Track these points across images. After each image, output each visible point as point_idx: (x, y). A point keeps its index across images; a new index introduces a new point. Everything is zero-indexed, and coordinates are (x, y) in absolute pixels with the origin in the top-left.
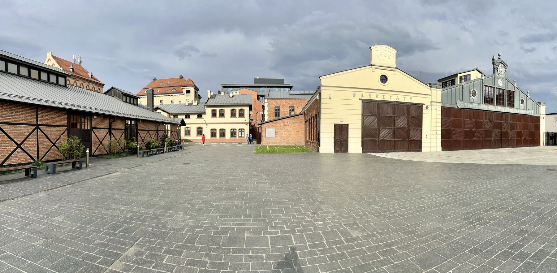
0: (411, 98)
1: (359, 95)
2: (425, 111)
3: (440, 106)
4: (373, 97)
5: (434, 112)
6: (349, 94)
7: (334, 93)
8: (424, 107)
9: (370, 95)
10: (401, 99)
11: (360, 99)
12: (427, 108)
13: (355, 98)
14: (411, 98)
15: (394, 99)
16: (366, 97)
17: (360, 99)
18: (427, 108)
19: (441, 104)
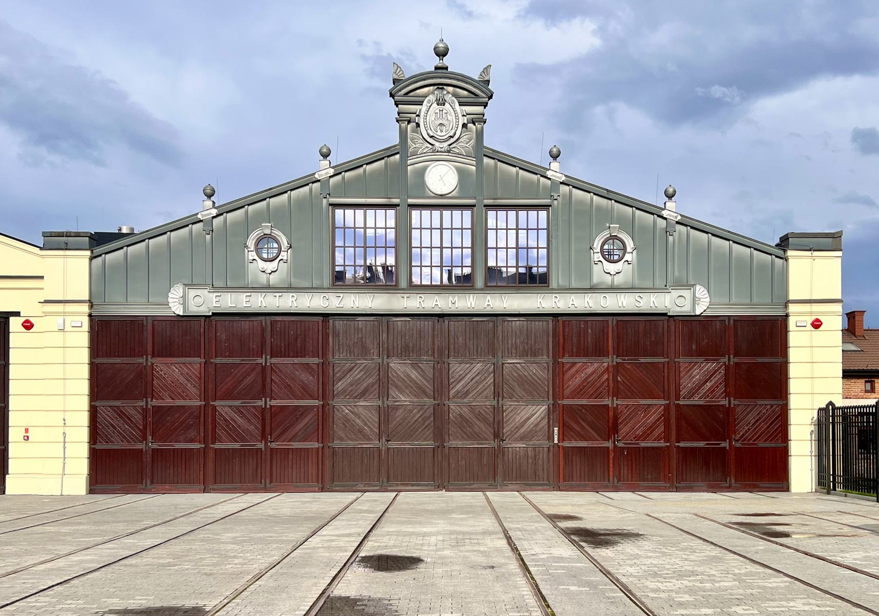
3: (80, 318)
8: (15, 324)
12: (28, 325)
18: (28, 325)
19: (85, 308)
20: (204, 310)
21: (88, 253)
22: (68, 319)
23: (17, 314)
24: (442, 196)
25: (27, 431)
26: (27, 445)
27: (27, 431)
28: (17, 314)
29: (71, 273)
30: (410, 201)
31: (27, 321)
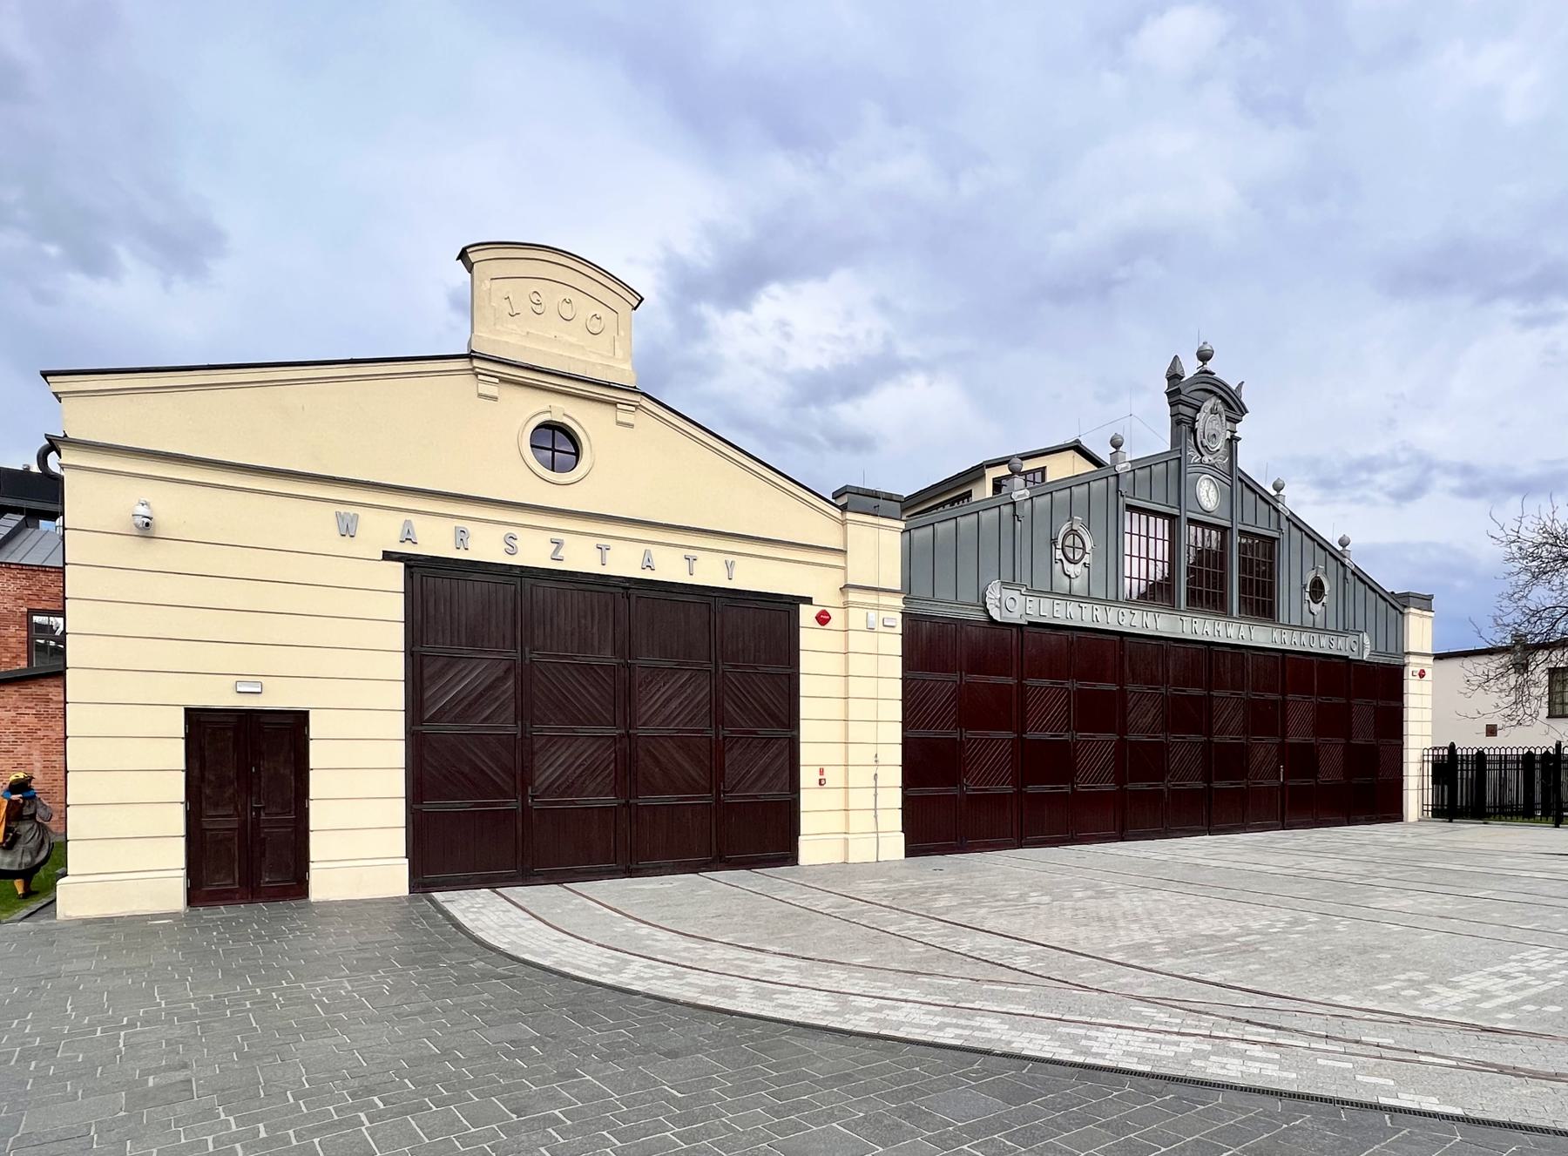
0: (729, 566)
1: (383, 528)
2: (810, 636)
3: (892, 611)
4: (486, 546)
5: (858, 641)
6: (307, 521)
7: (171, 503)
8: (807, 614)
9: (462, 537)
10: (670, 568)
11: (388, 556)
12: (823, 619)
13: (345, 546)
14: (729, 566)
15: (624, 562)
16: (436, 540)
17: (388, 556)
18: (823, 619)
20: (1015, 617)
21: (902, 525)
22: (883, 614)
23: (808, 601)
24: (1207, 513)
25: (822, 772)
26: (822, 792)
27: (822, 772)
28: (808, 601)
29: (878, 549)
30: (1190, 515)
31: (824, 613)
